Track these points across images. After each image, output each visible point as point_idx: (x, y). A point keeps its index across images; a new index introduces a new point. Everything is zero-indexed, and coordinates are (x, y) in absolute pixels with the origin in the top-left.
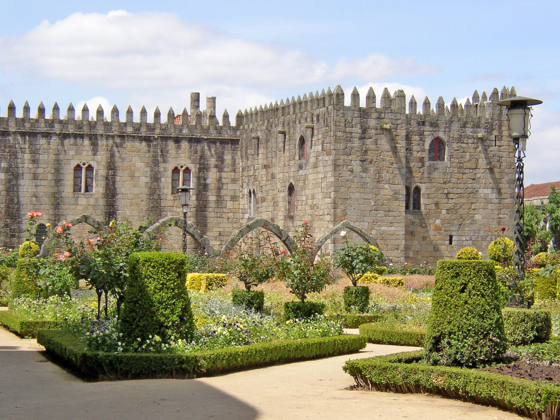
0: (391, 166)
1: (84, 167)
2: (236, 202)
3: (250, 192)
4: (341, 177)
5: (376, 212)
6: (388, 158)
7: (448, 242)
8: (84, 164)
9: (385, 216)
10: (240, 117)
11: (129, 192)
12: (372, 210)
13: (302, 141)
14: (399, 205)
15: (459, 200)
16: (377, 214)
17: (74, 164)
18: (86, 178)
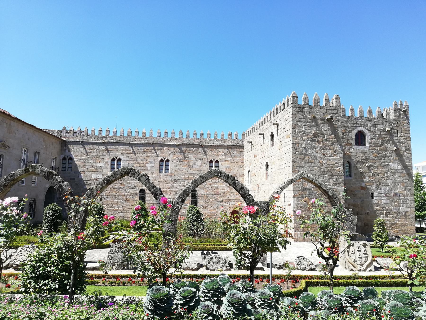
0: (332, 145)
1: (164, 160)
2: (242, 178)
3: (248, 172)
4: (297, 152)
5: (323, 176)
6: (330, 140)
7: (370, 198)
8: (165, 159)
9: (330, 179)
10: (243, 135)
11: (187, 173)
12: (320, 175)
13: (272, 136)
14: (339, 171)
15: (376, 171)
16: (323, 177)
17: (160, 158)
18: (166, 166)
